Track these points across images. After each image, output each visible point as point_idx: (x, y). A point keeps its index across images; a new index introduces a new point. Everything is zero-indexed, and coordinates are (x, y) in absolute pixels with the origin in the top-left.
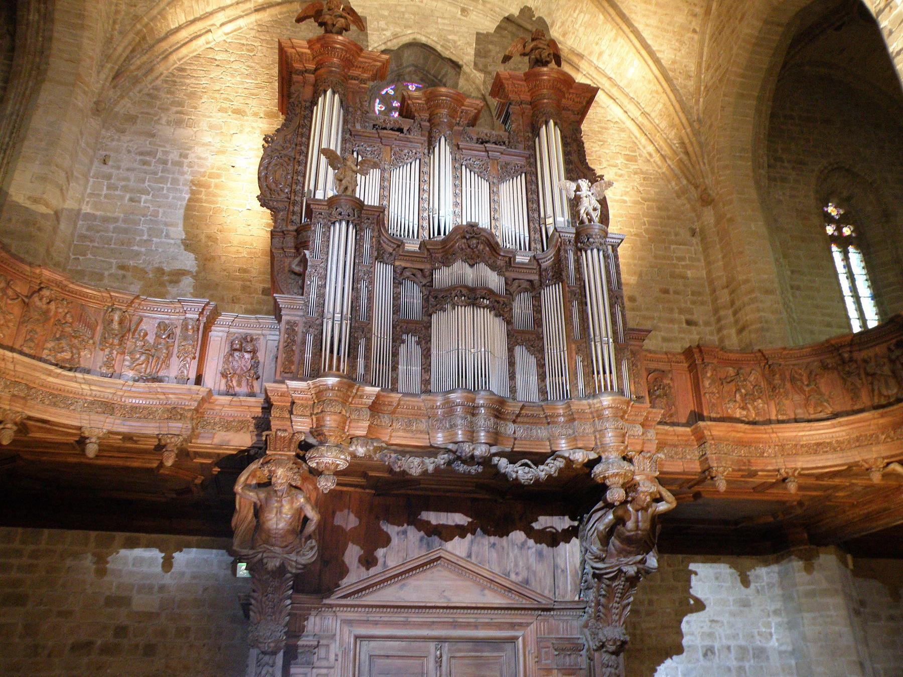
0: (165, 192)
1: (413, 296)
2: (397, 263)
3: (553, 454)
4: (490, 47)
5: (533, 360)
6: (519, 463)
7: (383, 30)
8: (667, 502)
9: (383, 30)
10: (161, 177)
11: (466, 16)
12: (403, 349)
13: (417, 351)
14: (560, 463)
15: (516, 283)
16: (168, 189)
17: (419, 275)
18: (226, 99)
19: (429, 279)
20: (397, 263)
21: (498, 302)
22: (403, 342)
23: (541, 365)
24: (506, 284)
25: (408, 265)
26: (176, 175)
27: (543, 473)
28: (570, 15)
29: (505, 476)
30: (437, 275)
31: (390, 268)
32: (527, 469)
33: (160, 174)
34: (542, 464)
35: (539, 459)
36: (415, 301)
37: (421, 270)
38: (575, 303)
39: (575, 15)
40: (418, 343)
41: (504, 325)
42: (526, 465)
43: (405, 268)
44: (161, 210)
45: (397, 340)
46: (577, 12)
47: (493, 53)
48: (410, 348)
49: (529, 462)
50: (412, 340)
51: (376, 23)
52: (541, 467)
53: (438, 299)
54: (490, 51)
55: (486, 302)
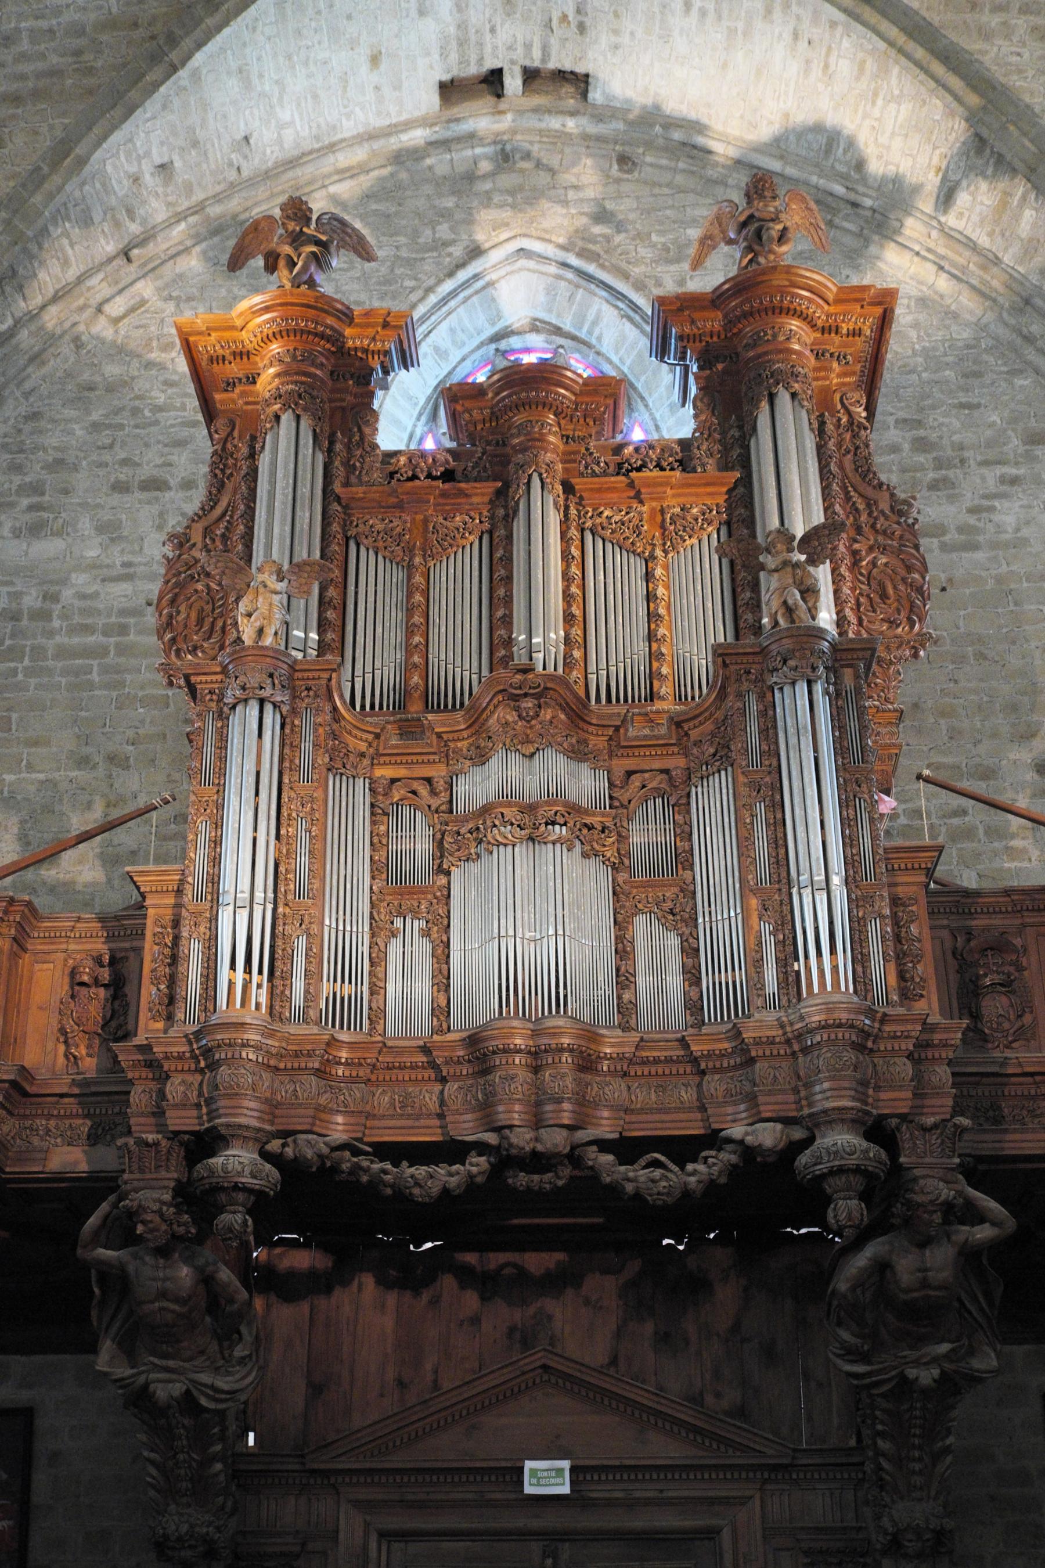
0: (20, 677)
2: (378, 772)
3: (713, 1139)
5: (673, 941)
6: (642, 1162)
7: (446, 244)
8: (994, 1224)
9: (446, 244)
10: (11, 649)
11: (629, 172)
12: (395, 949)
13: (421, 949)
14: (729, 1156)
15: (636, 781)
16: (29, 672)
17: (423, 791)
18: (125, 462)
19: (444, 797)
20: (378, 772)
21: (590, 828)
23: (690, 951)
24: (611, 784)
25: (401, 772)
26: (40, 640)
27: (693, 1179)
28: (866, 116)
29: (614, 1190)
30: (462, 788)
32: (658, 1173)
33: (8, 642)
34: (694, 1160)
35: (682, 1149)
36: (418, 847)
37: (429, 780)
38: (760, 809)
39: (876, 112)
40: (426, 933)
42: (656, 1164)
43: (393, 781)
44: (14, 716)
46: (880, 102)
49: (662, 1158)
51: (428, 232)
52: (690, 1167)
53: (464, 836)
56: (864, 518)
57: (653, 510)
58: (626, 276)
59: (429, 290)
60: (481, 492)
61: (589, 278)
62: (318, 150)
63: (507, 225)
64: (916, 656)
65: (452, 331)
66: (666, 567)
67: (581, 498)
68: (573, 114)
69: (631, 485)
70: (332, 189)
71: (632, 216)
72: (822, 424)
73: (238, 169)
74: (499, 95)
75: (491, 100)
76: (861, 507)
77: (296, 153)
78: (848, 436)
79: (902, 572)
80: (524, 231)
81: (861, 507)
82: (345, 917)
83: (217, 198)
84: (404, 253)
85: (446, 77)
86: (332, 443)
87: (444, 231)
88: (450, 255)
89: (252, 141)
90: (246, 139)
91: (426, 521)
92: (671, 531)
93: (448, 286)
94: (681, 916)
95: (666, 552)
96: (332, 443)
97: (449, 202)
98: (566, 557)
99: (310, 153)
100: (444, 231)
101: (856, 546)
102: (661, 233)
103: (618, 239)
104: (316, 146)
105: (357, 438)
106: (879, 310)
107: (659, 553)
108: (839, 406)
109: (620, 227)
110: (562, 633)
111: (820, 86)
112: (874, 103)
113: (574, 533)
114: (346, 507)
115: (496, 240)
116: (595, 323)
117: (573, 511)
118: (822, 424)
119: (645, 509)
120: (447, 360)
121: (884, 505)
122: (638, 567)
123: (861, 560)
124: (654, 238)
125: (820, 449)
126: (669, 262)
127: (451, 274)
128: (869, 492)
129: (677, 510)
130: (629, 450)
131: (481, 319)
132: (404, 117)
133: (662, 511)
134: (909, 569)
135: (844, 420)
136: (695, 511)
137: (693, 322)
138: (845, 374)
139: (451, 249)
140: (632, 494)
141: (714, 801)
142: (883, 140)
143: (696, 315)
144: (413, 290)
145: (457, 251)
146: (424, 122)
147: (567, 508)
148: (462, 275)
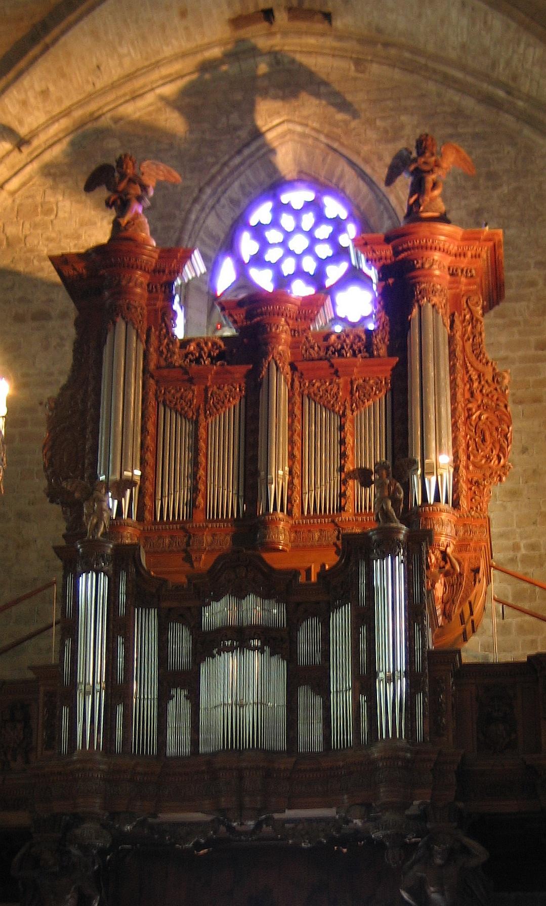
1: (182, 642)
4: (404, 118)
5: (318, 701)
7: (236, 128)
11: (363, 72)
12: (171, 705)
13: (186, 707)
22: (171, 698)
31: (153, 613)
37: (189, 608)
39: (521, 50)
40: (187, 697)
41: (283, 665)
43: (170, 610)
45: (164, 698)
47: (407, 131)
48: (178, 704)
50: (180, 695)
51: (224, 120)
53: (208, 644)
54: (402, 127)
55: (256, 643)
56: (476, 384)
57: (346, 382)
58: (358, 153)
59: (225, 164)
60: (240, 371)
61: (335, 150)
62: (146, 67)
63: (278, 113)
64: (501, 480)
65: (242, 187)
66: (352, 421)
67: (302, 374)
68: (323, 35)
69: (332, 366)
70: (159, 91)
71: (364, 106)
72: (452, 322)
73: (94, 84)
74: (271, 23)
75: (266, 24)
76: (475, 377)
77: (133, 69)
78: (469, 328)
79: (497, 424)
80: (289, 117)
81: (475, 377)
82: (144, 689)
83: (80, 104)
84: (208, 136)
85: (233, 17)
86: (148, 336)
87: (235, 118)
88: (239, 137)
89: (102, 68)
90: (98, 67)
91: (206, 390)
92: (357, 395)
93: (237, 160)
94: (322, 688)
95: (353, 411)
96: (148, 336)
97: (238, 96)
98: (291, 414)
99: (143, 68)
100: (235, 118)
101: (470, 406)
102: (383, 118)
103: (354, 124)
104: (147, 63)
105: (164, 330)
106: (491, 244)
107: (348, 412)
108: (465, 306)
109: (355, 114)
110: (287, 468)
111: (483, 33)
112: (518, 44)
113: (298, 399)
114: (157, 382)
115: (270, 125)
116: (341, 177)
117: (297, 383)
118: (452, 322)
119: (341, 381)
120: (239, 206)
121: (489, 377)
122: (336, 422)
123: (472, 415)
124: (378, 123)
125: (451, 339)
126: (388, 141)
127: (239, 152)
128: (480, 367)
129: (361, 381)
130: (333, 337)
131: (263, 175)
132: (206, 40)
133: (352, 383)
134: (501, 421)
135: (468, 317)
136: (371, 382)
137: (374, 251)
138: (469, 284)
139: (240, 133)
140: (333, 371)
141: (341, 620)
142: (528, 66)
143: (375, 248)
144: (213, 165)
145: (243, 134)
146: (221, 43)
147: (293, 380)
148: (246, 152)
